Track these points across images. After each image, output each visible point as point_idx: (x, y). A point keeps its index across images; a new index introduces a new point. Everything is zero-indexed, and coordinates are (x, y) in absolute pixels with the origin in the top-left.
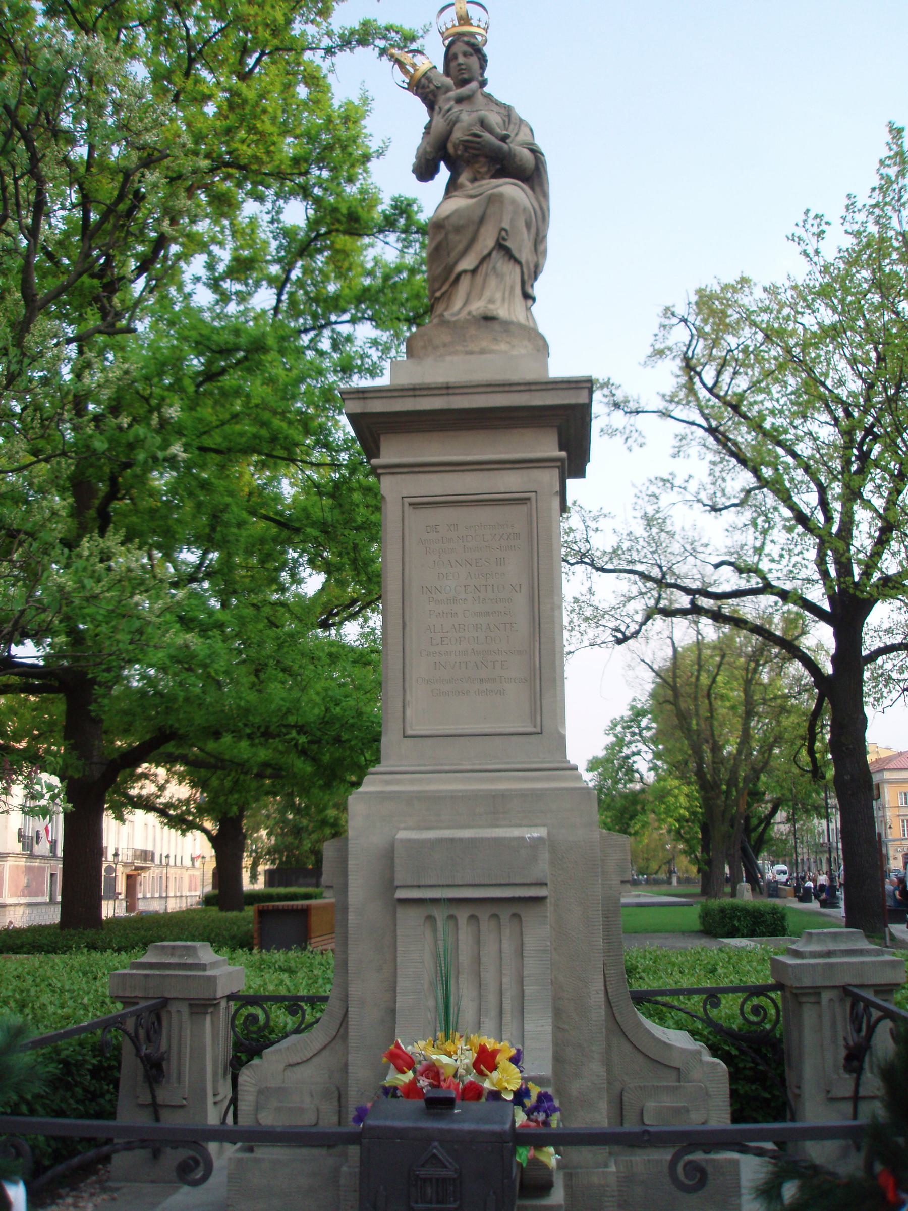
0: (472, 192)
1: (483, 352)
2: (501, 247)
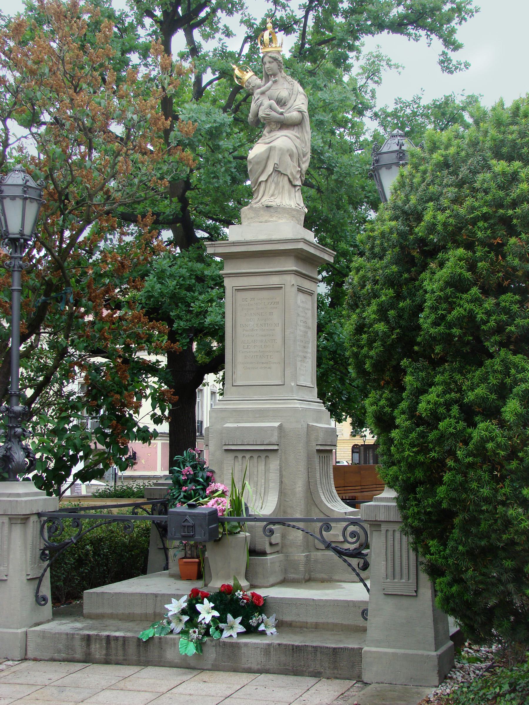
0: (267, 141)
2: (276, 170)
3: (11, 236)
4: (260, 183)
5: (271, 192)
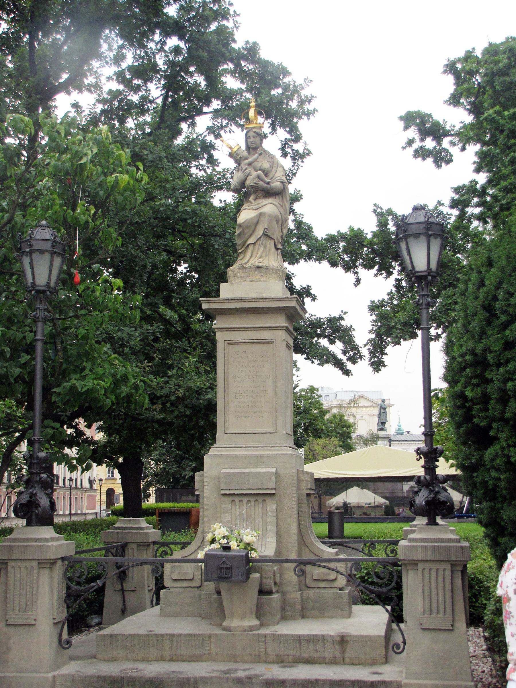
0: (255, 207)
1: (257, 281)
2: (266, 235)
3: (37, 288)
4: (248, 245)
5: (259, 254)
